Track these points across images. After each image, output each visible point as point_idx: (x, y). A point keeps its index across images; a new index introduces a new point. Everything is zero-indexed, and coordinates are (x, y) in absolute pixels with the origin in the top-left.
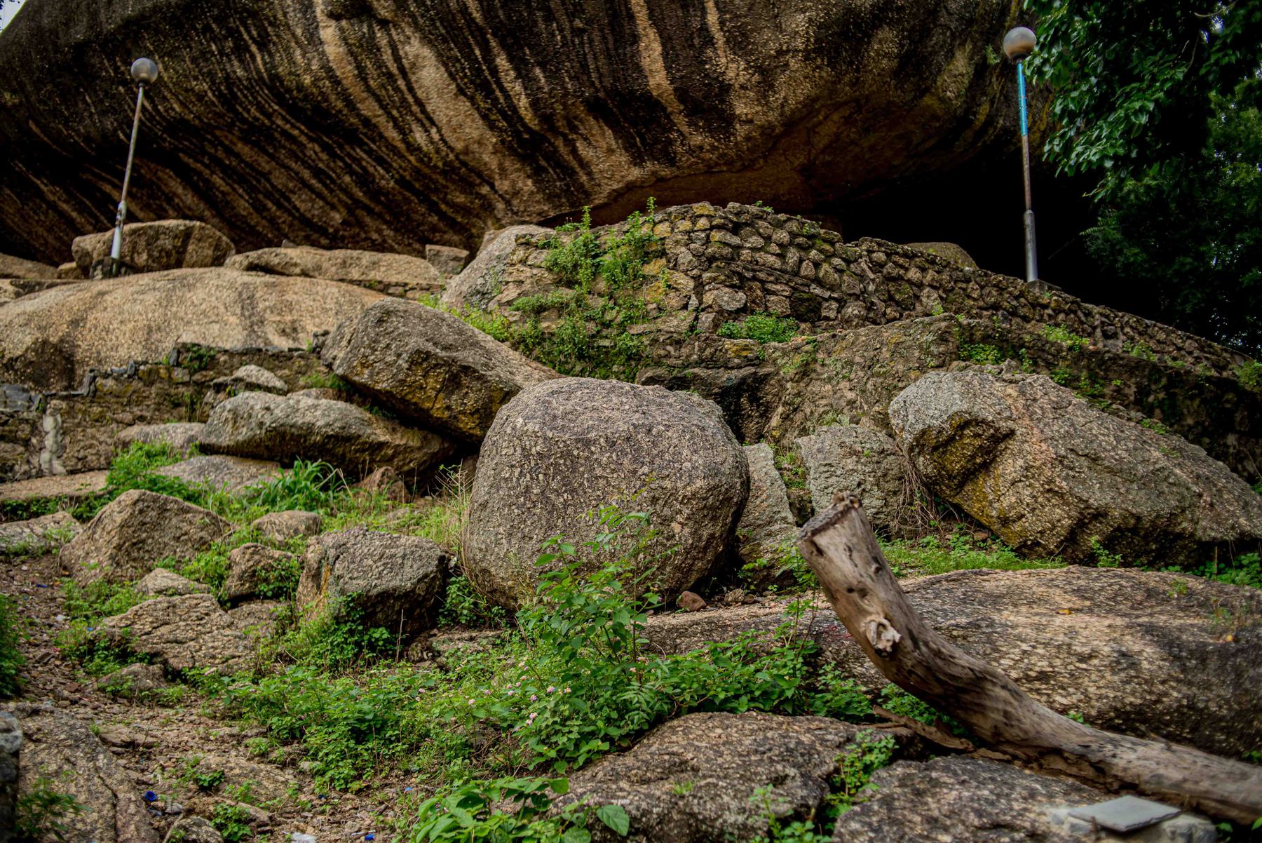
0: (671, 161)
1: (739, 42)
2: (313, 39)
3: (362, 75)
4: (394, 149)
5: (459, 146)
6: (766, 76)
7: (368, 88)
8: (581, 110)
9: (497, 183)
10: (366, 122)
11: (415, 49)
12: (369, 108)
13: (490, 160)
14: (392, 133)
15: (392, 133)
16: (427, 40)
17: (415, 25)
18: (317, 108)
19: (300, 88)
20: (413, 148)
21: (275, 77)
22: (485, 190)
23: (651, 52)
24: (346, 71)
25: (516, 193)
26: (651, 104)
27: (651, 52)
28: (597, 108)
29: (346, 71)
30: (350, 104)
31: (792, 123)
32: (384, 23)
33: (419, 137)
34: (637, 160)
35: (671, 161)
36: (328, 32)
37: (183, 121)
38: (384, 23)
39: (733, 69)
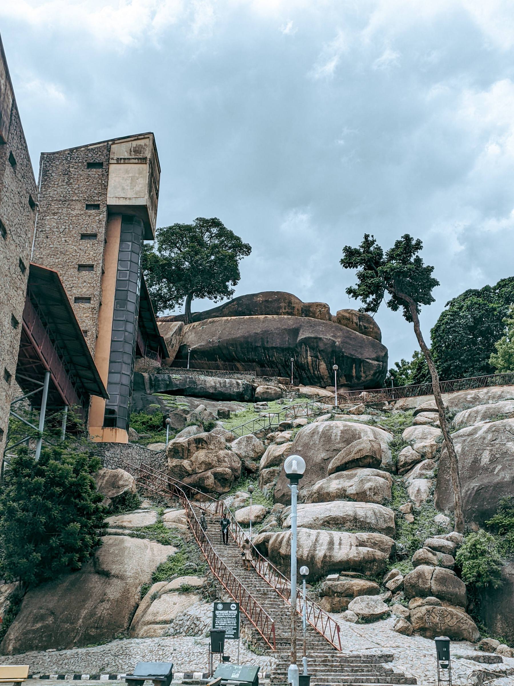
0: (351, 382)
1: (364, 372)
2: (307, 358)
3: (312, 364)
4: (311, 373)
5: (322, 375)
6: (367, 376)
7: (312, 366)
8: (343, 375)
9: (325, 380)
10: (309, 369)
11: (322, 363)
12: (311, 368)
13: (326, 377)
14: (312, 371)
15: (312, 371)
16: (325, 363)
17: (325, 361)
18: (302, 366)
19: (302, 363)
20: (314, 373)
21: (297, 360)
22: (321, 380)
23: (354, 371)
24: (310, 363)
25: (327, 381)
26: (353, 376)
27: (354, 371)
28: (345, 376)
29: (310, 363)
30: (308, 366)
31: (367, 381)
32: (319, 359)
33: (316, 372)
34: (347, 381)
35: (351, 382)
36: (309, 358)
37: (274, 361)
38: (319, 359)
39: (363, 375)
